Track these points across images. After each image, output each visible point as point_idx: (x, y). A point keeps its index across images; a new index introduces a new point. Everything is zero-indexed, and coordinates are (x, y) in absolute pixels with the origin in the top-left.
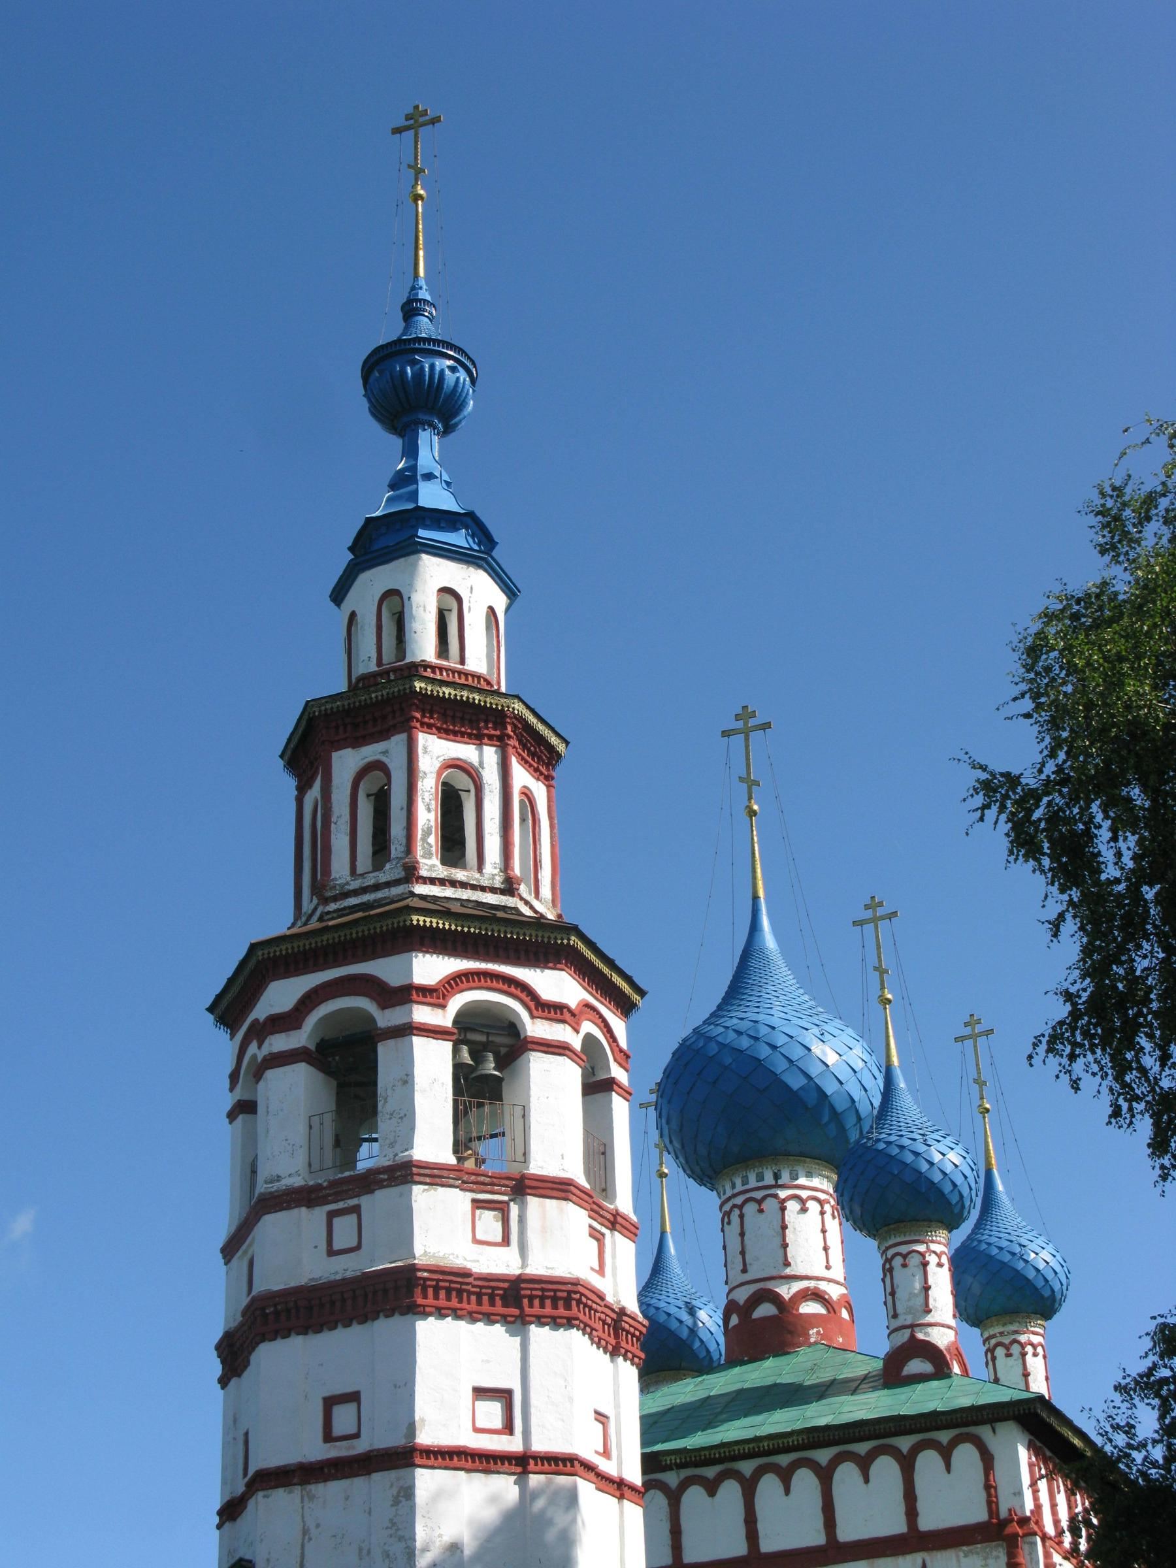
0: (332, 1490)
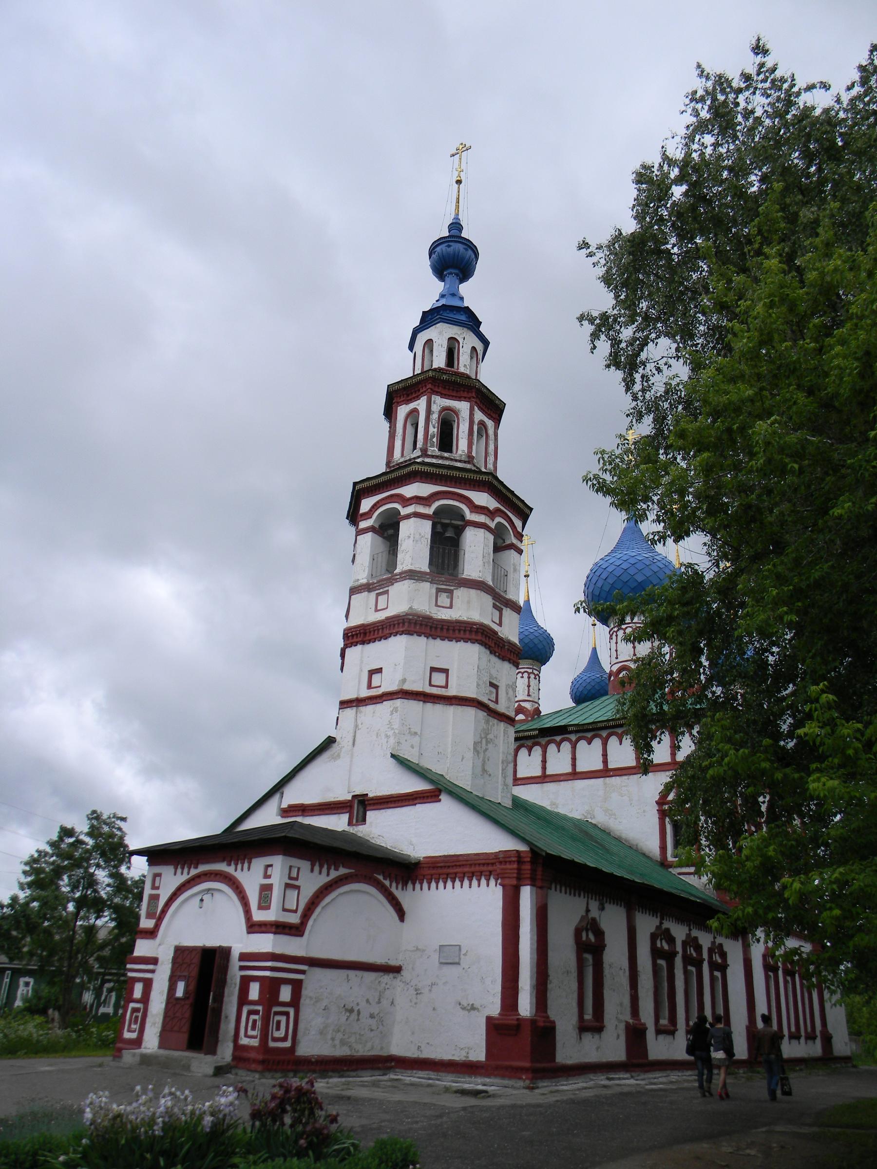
0: (369, 709)
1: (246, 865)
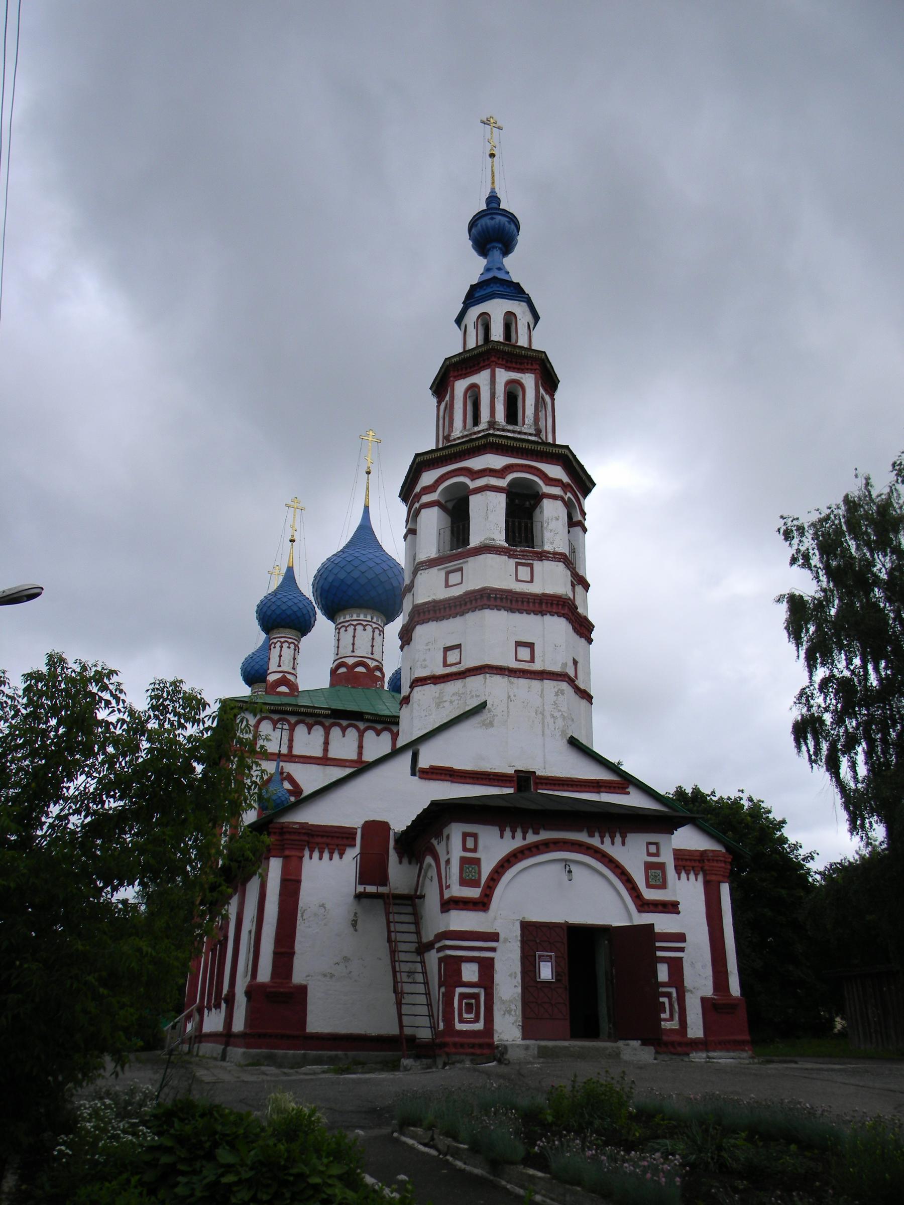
0: (523, 682)
1: (618, 839)
